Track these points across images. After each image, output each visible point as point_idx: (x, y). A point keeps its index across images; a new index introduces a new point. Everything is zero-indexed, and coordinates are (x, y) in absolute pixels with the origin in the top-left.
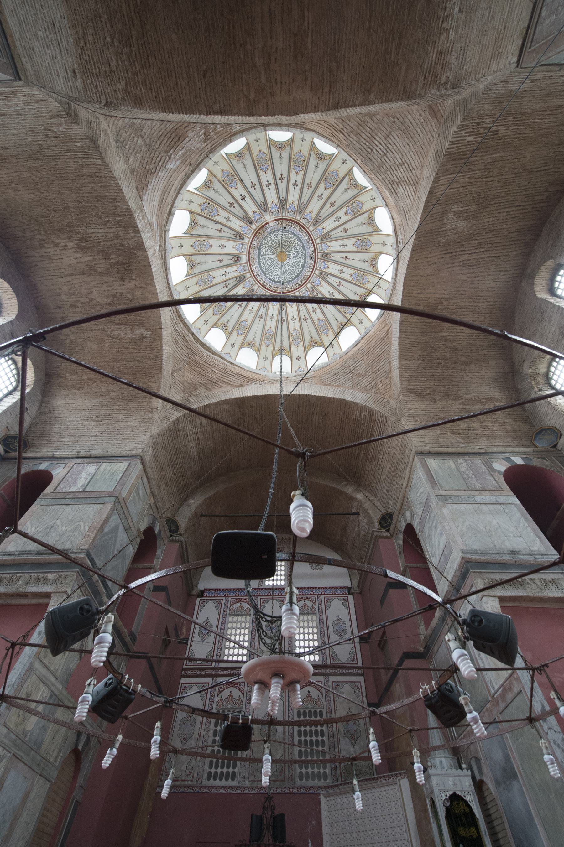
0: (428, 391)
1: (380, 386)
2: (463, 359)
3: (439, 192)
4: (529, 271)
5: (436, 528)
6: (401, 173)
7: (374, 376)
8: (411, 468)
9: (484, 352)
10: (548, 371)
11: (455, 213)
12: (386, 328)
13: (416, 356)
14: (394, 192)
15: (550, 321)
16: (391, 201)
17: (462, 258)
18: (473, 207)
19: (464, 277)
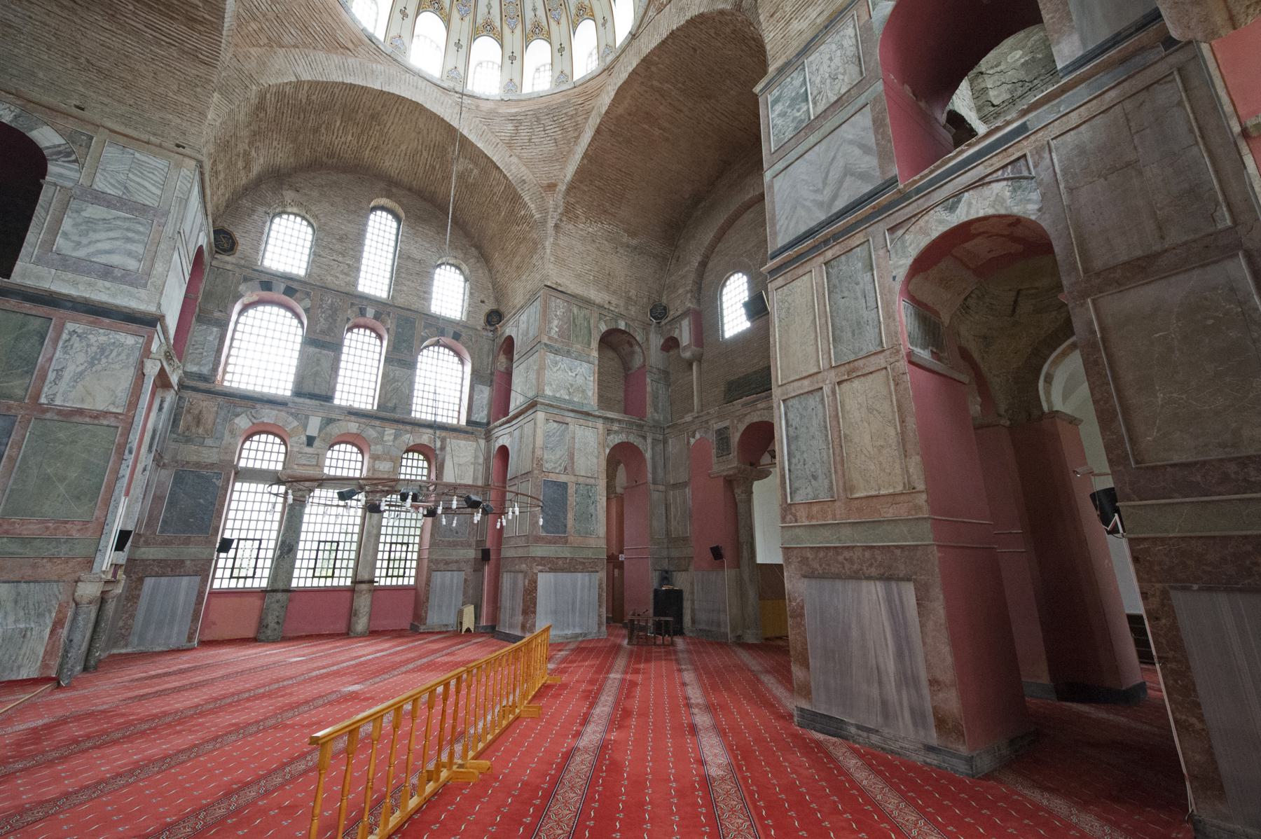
0: (262, 115)
1: (254, 25)
2: (301, 137)
3: (495, 173)
4: (394, 190)
5: (128, 240)
6: (524, 133)
7: (271, 16)
8: (160, 146)
9: (307, 152)
10: (289, 214)
11: (471, 171)
12: (351, 46)
13: (314, 97)
14: (512, 118)
15: (349, 222)
16: (504, 110)
17: (425, 154)
18: (471, 180)
19: (403, 147)
